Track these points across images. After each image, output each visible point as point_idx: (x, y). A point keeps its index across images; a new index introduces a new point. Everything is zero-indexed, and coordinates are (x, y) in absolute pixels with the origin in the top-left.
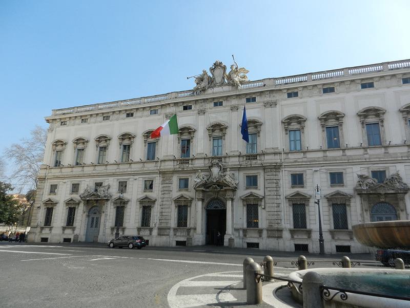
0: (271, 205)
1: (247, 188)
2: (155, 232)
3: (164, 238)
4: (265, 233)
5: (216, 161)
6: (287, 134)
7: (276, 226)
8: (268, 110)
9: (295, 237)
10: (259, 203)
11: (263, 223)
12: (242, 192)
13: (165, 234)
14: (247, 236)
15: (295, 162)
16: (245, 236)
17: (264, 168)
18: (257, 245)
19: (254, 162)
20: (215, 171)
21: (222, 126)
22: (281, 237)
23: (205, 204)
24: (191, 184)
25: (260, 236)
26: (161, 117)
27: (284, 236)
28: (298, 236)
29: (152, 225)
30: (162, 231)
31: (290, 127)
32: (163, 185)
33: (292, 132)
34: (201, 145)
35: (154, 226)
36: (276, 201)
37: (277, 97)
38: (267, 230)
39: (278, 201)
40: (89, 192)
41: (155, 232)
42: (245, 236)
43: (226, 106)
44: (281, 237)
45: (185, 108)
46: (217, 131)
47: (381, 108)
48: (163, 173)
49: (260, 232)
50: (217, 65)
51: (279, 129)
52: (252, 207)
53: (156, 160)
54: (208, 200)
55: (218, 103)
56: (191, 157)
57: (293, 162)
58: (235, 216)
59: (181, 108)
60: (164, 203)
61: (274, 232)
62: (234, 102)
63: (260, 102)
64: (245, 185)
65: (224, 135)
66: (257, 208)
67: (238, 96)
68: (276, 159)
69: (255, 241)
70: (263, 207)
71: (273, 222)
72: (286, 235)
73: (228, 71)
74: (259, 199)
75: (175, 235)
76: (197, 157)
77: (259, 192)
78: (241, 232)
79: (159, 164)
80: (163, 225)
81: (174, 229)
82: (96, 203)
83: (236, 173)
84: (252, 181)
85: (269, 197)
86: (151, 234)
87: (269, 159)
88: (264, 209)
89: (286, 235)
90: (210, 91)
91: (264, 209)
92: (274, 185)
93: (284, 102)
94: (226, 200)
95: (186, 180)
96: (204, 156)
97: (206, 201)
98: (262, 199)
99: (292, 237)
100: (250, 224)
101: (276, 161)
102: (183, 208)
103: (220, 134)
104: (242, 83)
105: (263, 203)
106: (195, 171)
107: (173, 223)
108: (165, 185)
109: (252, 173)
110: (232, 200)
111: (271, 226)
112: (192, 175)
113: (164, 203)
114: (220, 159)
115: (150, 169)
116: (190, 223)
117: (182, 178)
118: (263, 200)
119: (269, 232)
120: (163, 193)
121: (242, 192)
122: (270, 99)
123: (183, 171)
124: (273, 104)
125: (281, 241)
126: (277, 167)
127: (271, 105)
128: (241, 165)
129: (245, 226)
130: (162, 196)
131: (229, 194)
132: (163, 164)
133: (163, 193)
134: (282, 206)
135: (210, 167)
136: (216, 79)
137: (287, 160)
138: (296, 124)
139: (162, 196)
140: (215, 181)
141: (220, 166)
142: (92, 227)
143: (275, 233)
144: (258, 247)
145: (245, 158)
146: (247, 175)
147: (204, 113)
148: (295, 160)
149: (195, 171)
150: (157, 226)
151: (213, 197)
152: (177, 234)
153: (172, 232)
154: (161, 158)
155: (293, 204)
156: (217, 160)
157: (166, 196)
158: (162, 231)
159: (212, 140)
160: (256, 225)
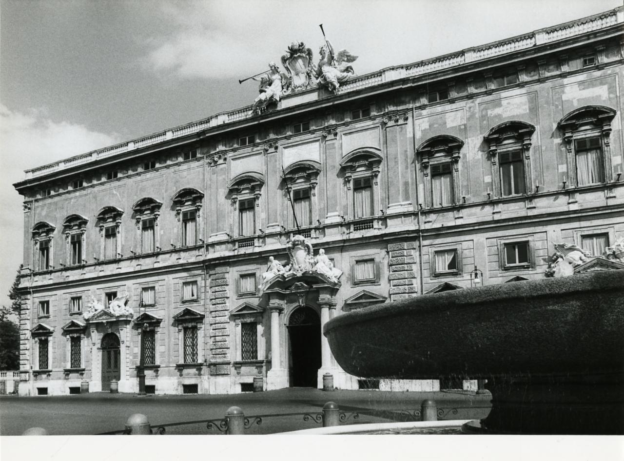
5: (300, 237)
23: (286, 319)
32: (214, 289)
40: (96, 310)
43: (315, 131)
47: (603, 107)
50: (296, 53)
73: (316, 59)
82: (111, 327)
94: (320, 306)
104: (343, 83)
107: (235, 354)
108: (217, 289)
114: (306, 232)
131: (324, 297)
141: (308, 246)
142: (109, 367)
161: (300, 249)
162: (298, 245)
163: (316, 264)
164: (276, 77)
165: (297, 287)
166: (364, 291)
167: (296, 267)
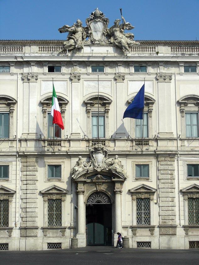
0: (165, 199)
1: (137, 180)
2: (16, 233)
3: (31, 241)
4: (157, 230)
5: (100, 145)
6: (183, 117)
7: (170, 223)
8: (162, 85)
9: (190, 233)
10: (151, 197)
11: (155, 221)
12: (130, 184)
13: (33, 235)
14: (137, 235)
15: (192, 151)
16: (134, 234)
17: (156, 155)
18: (149, 244)
19: (145, 148)
20: (100, 157)
21: (105, 100)
22: (175, 235)
24: (66, 173)
25: (152, 234)
26: (15, 77)
27: (177, 234)
28: (192, 233)
29: (11, 224)
30: (26, 231)
31: (186, 109)
32: (25, 173)
33: (188, 116)
34: (77, 122)
35: (13, 225)
36: (171, 195)
37: (173, 70)
38: (159, 227)
39: (171, 195)
41: (16, 233)
42: (134, 234)
44: (175, 235)
45: (51, 70)
46: (98, 104)
48: (24, 156)
49: (152, 229)
51: (174, 109)
52: (143, 198)
53: (11, 138)
54: (89, 193)
55: (98, 66)
56: (63, 137)
57: (190, 151)
58: (125, 212)
59: (46, 69)
60: (29, 196)
61: (167, 229)
62: (122, 70)
63: (152, 74)
64: (135, 176)
65: (107, 111)
66: (149, 202)
67: (127, 64)
68: (171, 146)
69: (147, 239)
70: (155, 201)
71: (167, 218)
72: (180, 231)
74: (150, 192)
75: (45, 236)
76: (72, 137)
77: (152, 184)
78: (130, 230)
79: (14, 144)
80: (29, 224)
81: (43, 229)
83: (123, 161)
84: (143, 171)
85: (163, 190)
86: (10, 236)
87: (163, 146)
88: (156, 203)
89: (180, 231)
90: (87, 51)
91: (156, 203)
92: (169, 176)
93: (178, 77)
95: (58, 167)
96: (81, 137)
97: (87, 194)
98: (154, 192)
99: (187, 234)
100: (139, 220)
101: (171, 149)
102: (54, 200)
103: (102, 109)
105: (155, 197)
106: (69, 156)
107: (41, 220)
109: (142, 161)
110: (120, 192)
111: (165, 222)
112: (64, 160)
113: (29, 196)
114: (103, 141)
115: (3, 150)
116: (67, 220)
117: (51, 164)
118: (156, 194)
119: (163, 229)
120: (25, 182)
121: (130, 184)
122: (163, 72)
123: (53, 155)
124: (167, 78)
125: (174, 239)
126: (172, 155)
127: (165, 80)
128: (130, 151)
129: (135, 224)
130: (24, 187)
132: (23, 143)
133: (25, 182)
134: (176, 200)
135: (92, 152)
136: (94, 33)
137: (183, 148)
138: (193, 105)
139: (24, 187)
140: (99, 170)
143: (168, 229)
144: (150, 246)
145: (134, 143)
146: (137, 164)
147: (79, 80)
148: (192, 148)
149: (69, 156)
150: (18, 226)
151: (95, 189)
152: (48, 235)
153: (40, 233)
154: (19, 137)
155: (188, 198)
156: (97, 144)
157: (30, 187)
158: (26, 231)
159: (91, 117)
160: (148, 220)
161: (100, 153)
162: (99, 150)
163: (112, 164)
164: (80, 29)
165: (98, 178)
166: (143, 185)
167: (96, 164)
